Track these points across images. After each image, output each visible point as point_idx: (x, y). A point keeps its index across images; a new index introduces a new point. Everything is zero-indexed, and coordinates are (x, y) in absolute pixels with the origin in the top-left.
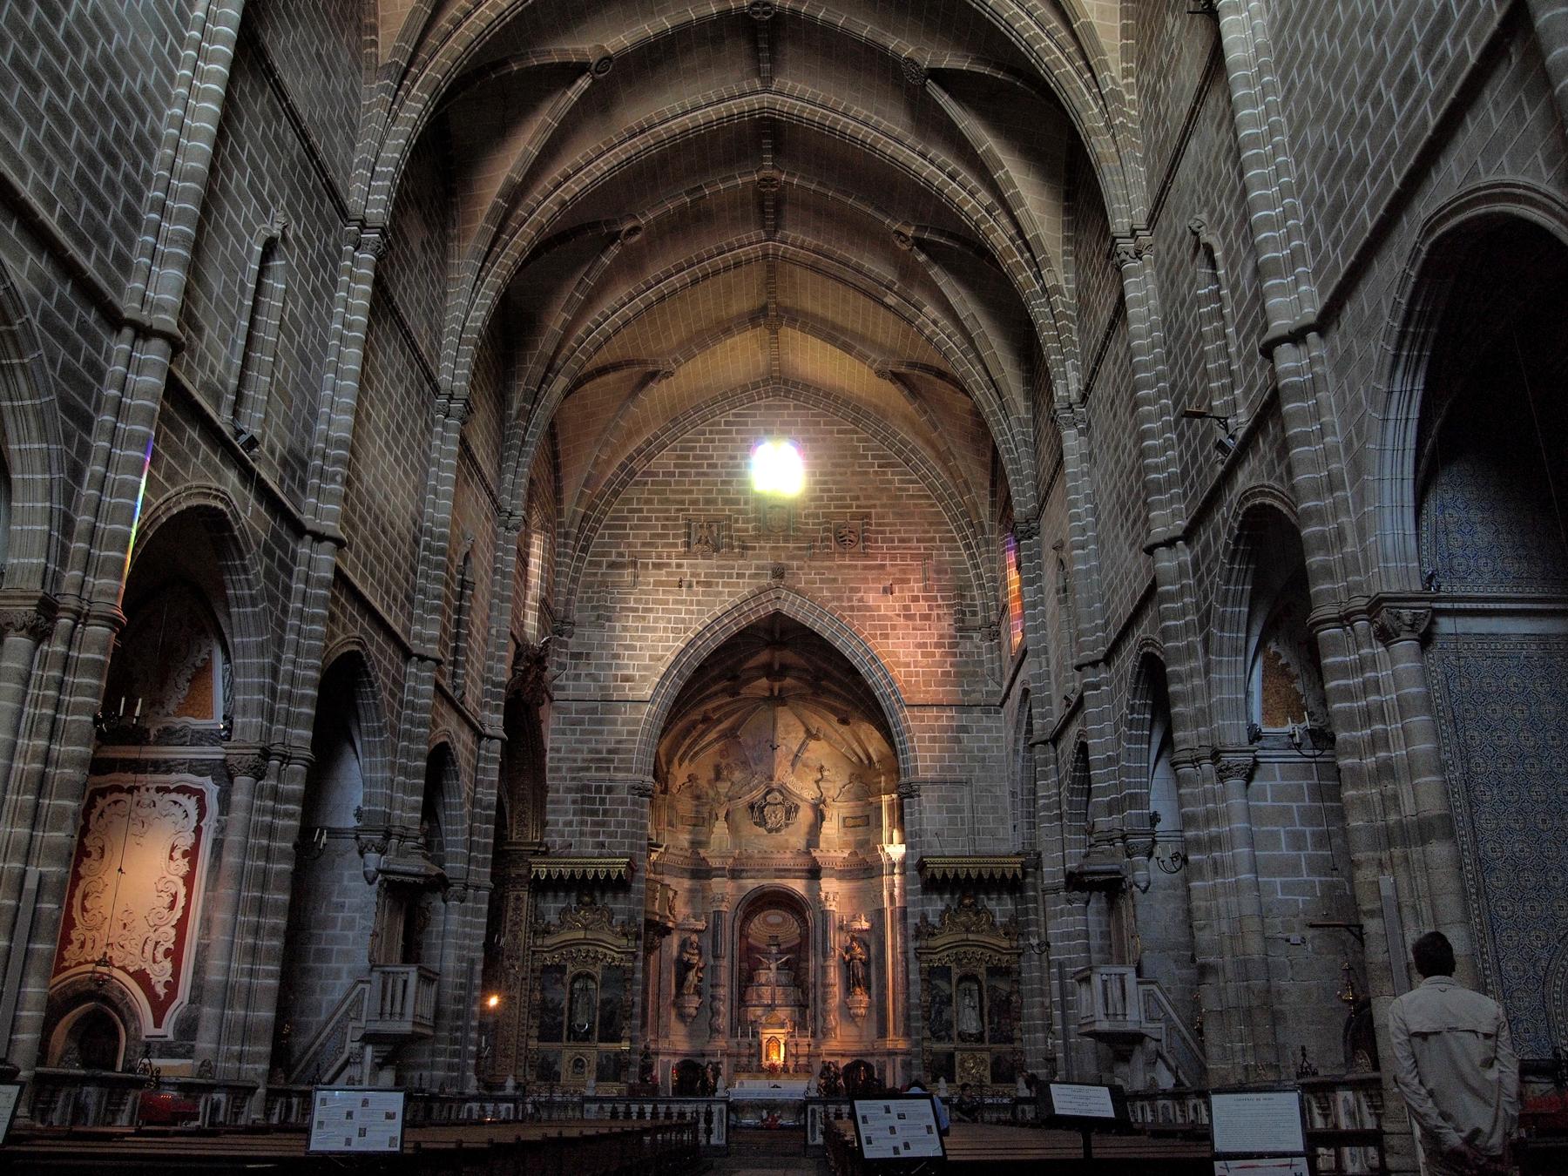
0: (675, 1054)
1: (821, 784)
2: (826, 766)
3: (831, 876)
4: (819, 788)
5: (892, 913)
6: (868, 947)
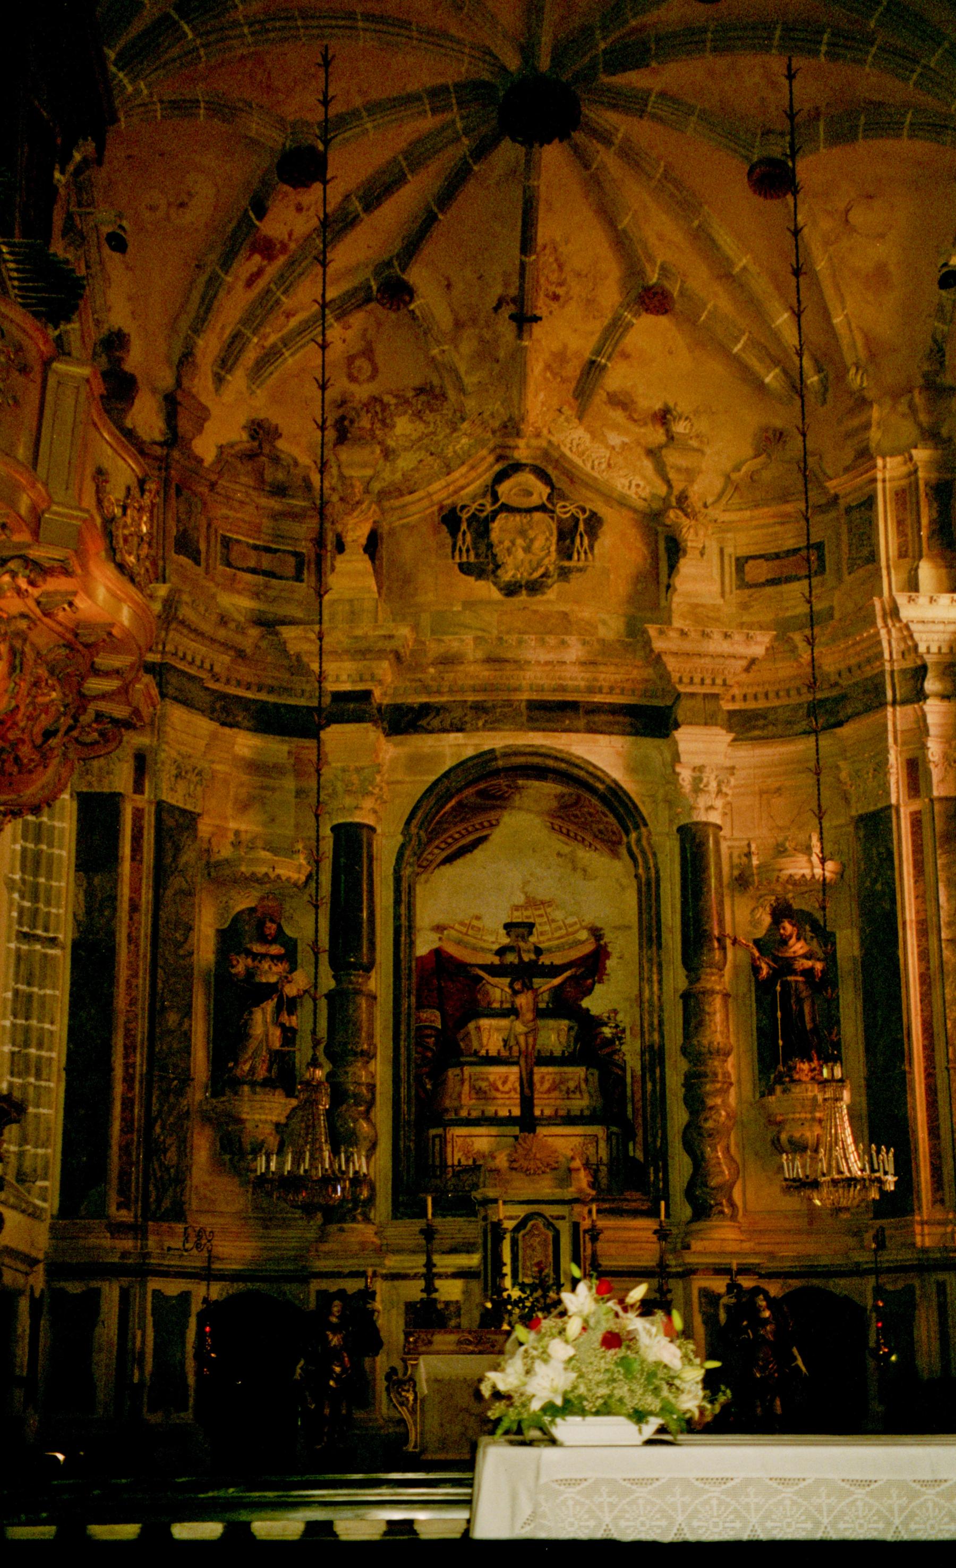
0: (207, 1275)
1: (672, 458)
2: (683, 406)
3: (709, 721)
4: (661, 470)
5: (916, 823)
6: (824, 935)
